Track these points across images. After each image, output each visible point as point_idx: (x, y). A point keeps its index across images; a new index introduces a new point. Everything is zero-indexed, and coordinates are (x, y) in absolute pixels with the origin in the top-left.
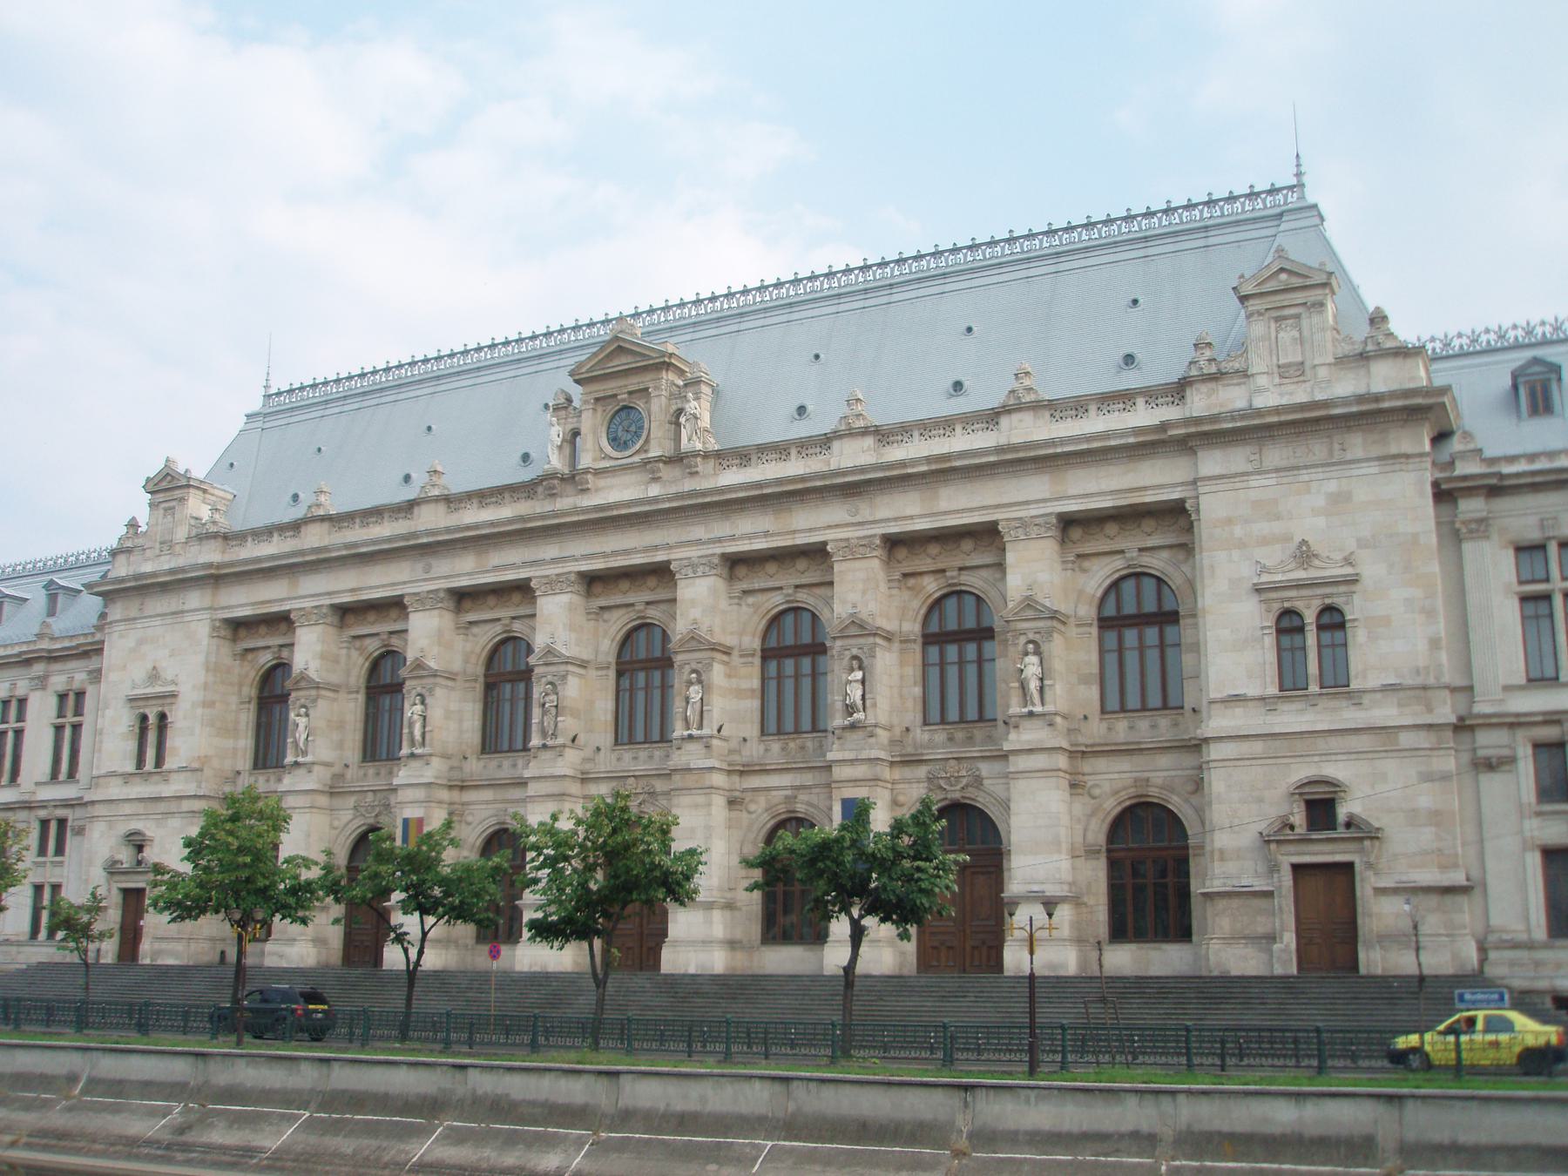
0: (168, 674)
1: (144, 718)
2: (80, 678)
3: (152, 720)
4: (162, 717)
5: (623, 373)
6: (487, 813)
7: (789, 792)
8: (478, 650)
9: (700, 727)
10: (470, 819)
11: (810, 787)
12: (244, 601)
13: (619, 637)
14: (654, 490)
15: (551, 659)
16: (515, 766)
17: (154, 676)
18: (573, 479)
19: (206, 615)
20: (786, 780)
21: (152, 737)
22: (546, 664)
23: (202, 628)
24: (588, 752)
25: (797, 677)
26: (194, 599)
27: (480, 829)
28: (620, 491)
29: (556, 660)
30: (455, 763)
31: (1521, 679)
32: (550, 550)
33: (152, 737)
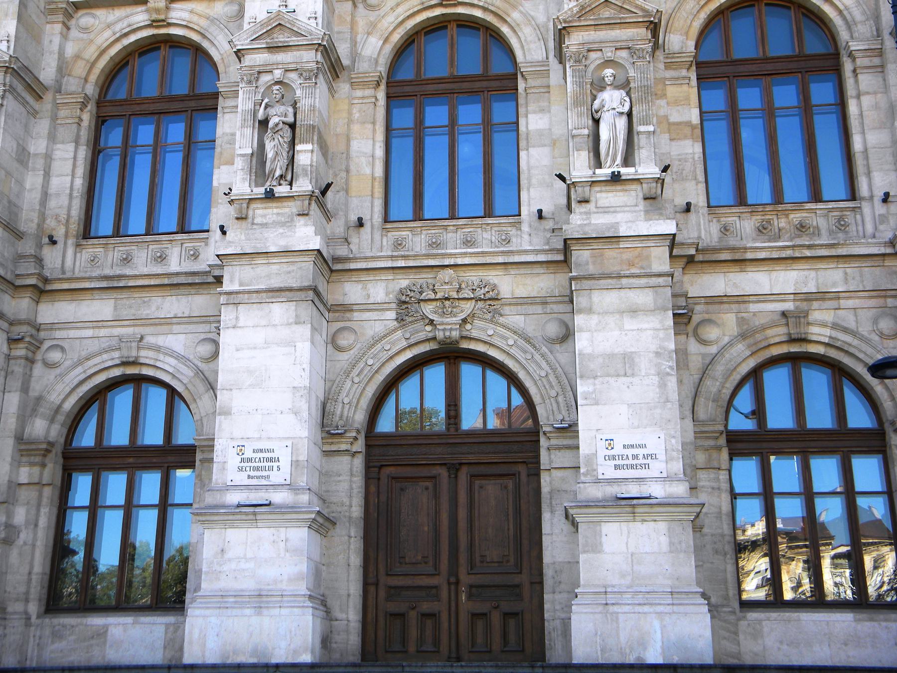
6: (93, 346)
7: (789, 306)
8: (91, 53)
9: (628, 161)
10: (55, 356)
11: (837, 295)
13: (396, 37)
15: (281, 38)
16: (162, 258)
20: (787, 280)
22: (273, 49)
24: (338, 227)
25: (769, 113)
27: (77, 374)
29: (294, 40)
30: (27, 247)
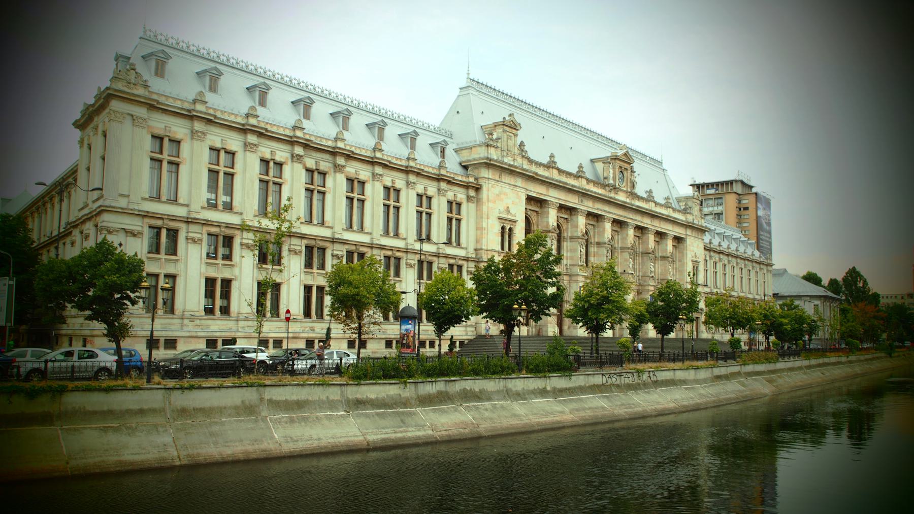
0: (512, 211)
1: (503, 228)
2: (324, 166)
3: (507, 230)
4: (510, 229)
5: (624, 161)
12: (538, 191)
14: (628, 201)
17: (508, 210)
18: (615, 188)
19: (524, 191)
21: (507, 237)
23: (524, 198)
26: (519, 182)
28: (621, 197)
31: (147, 196)
32: (607, 208)
33: (507, 237)
